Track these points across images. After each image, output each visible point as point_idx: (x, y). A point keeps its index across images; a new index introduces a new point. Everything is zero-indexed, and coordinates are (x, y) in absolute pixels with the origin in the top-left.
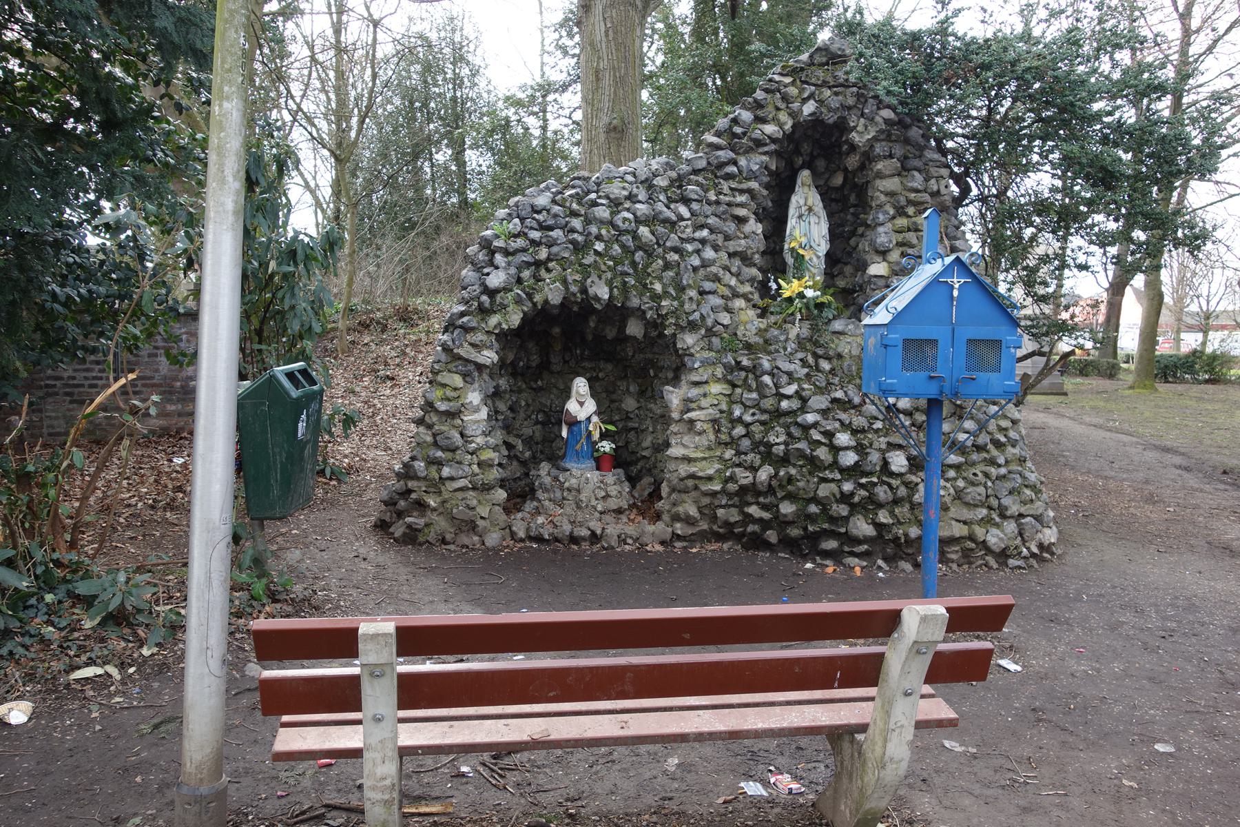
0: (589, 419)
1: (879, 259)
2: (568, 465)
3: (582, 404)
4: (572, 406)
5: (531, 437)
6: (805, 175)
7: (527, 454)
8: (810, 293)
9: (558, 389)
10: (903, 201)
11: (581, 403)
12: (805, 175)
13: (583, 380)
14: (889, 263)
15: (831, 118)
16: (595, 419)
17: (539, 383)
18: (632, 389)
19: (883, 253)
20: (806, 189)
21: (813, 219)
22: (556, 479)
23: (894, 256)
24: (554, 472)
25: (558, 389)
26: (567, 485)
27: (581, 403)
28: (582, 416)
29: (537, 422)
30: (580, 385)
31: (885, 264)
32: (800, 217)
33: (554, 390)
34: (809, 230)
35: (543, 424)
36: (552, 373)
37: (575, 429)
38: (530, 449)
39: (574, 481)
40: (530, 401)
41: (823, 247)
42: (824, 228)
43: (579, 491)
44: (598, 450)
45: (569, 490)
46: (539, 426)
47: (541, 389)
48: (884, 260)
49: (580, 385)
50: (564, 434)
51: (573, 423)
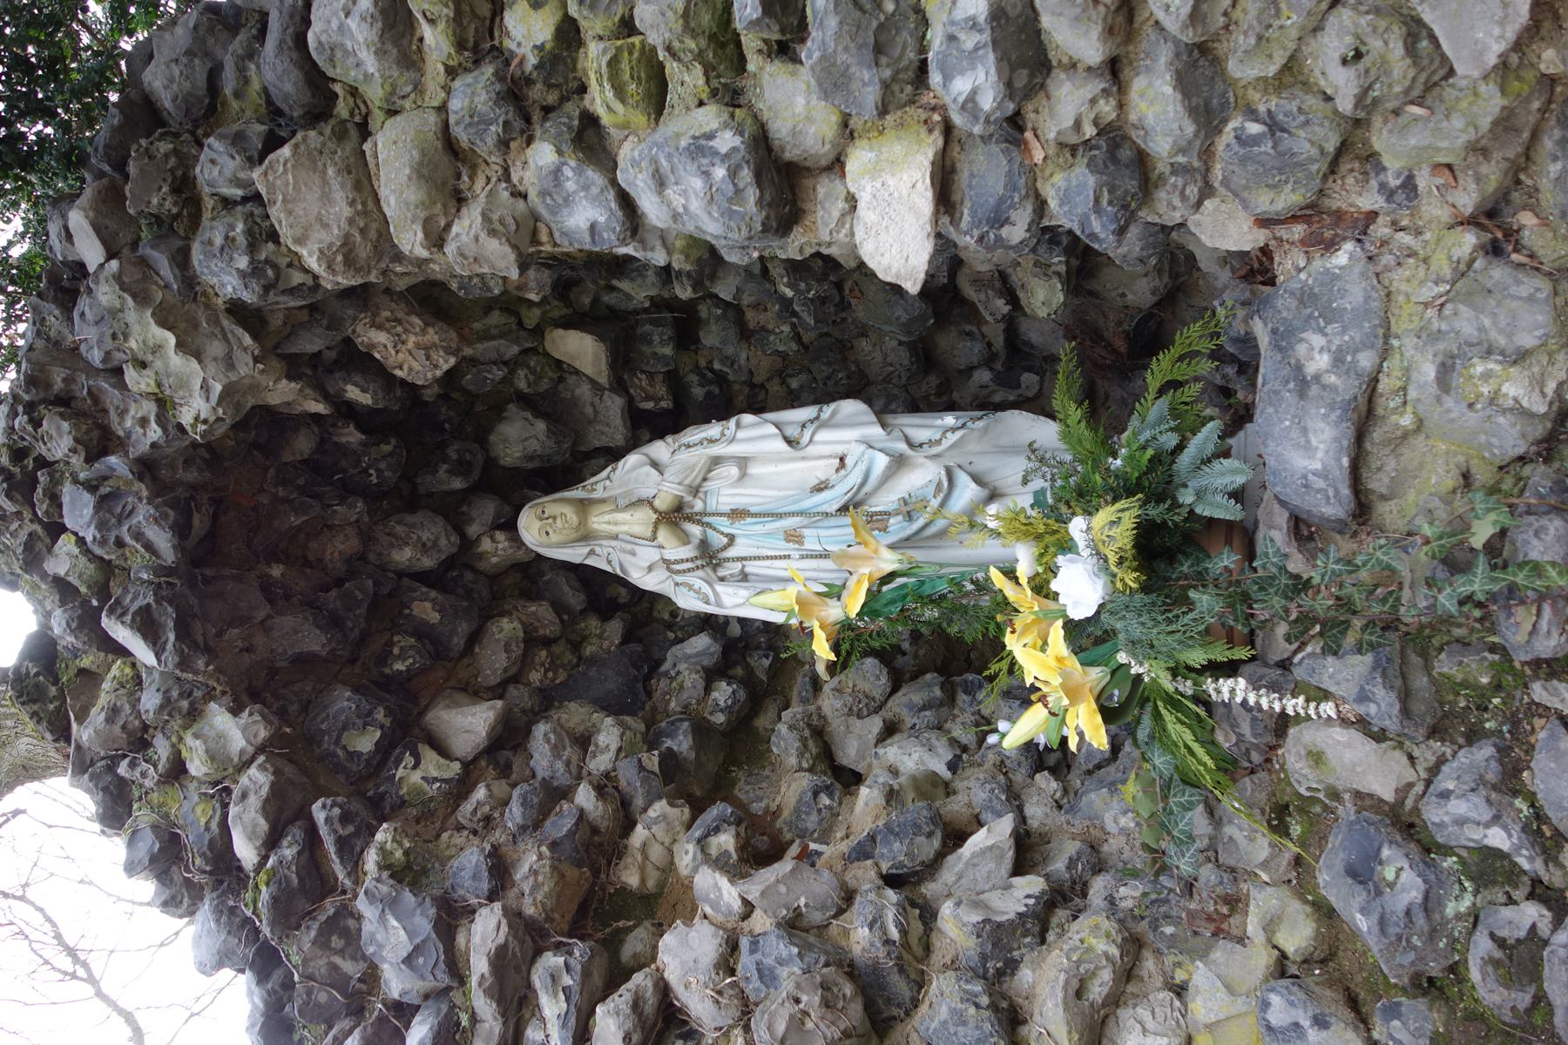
1: (826, 201)
6: (544, 529)
8: (1081, 589)
10: (473, 95)
12: (544, 529)
14: (848, 132)
15: (154, 535)
19: (784, 181)
20: (600, 521)
21: (724, 493)
23: (793, 103)
31: (858, 159)
32: (709, 557)
34: (773, 518)
41: (846, 437)
42: (752, 435)
48: (837, 165)
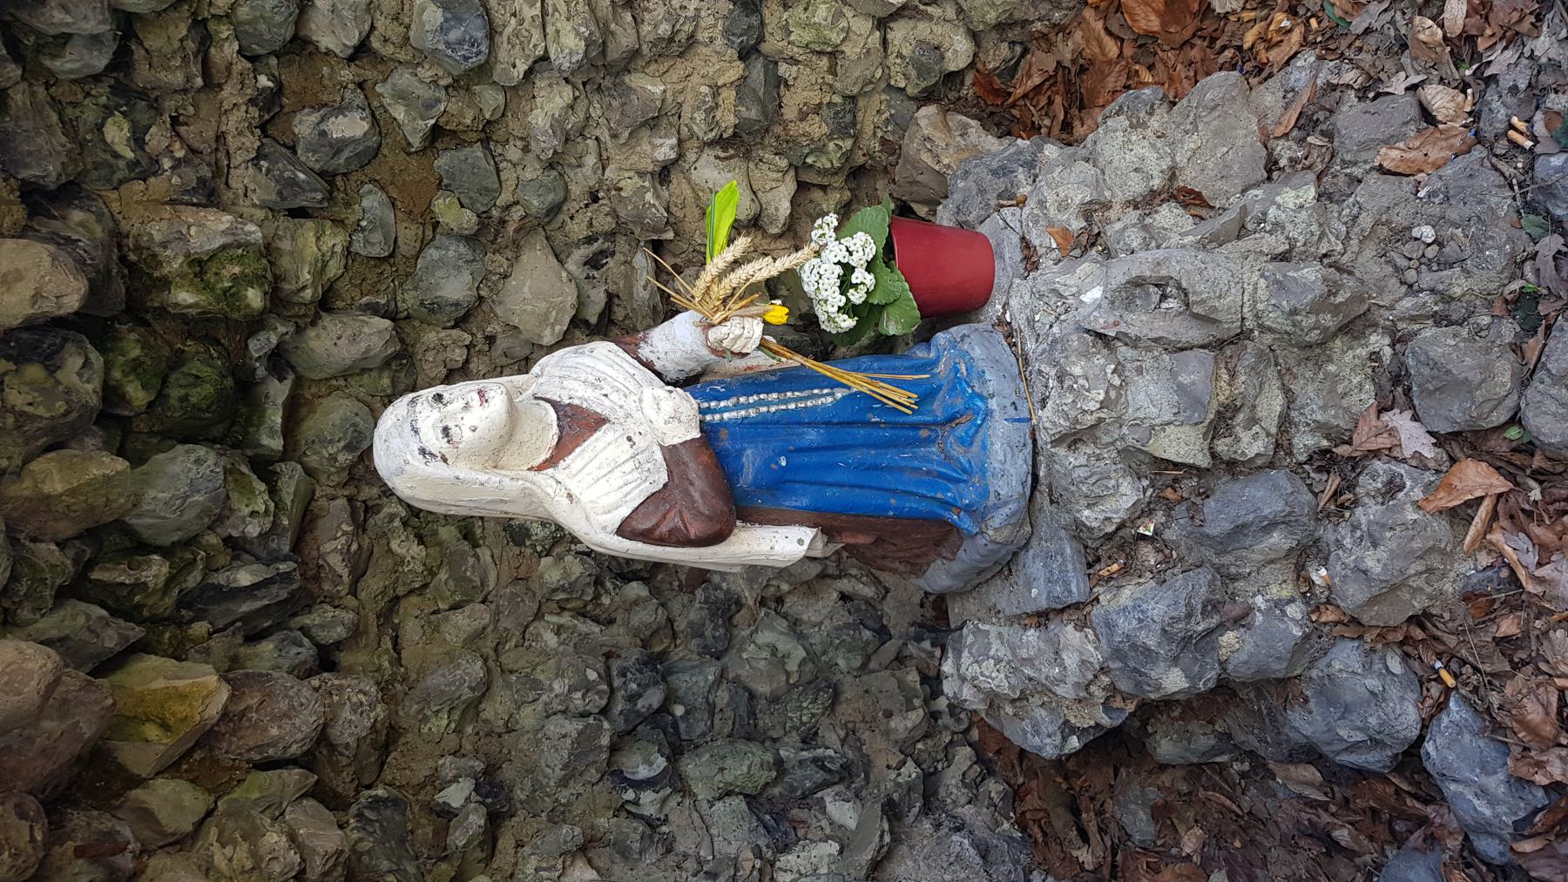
0: (688, 382)
2: (1004, 467)
3: (577, 424)
4: (598, 493)
5: (750, 799)
7: (842, 811)
9: (485, 689)
11: (568, 441)
13: (394, 415)
16: (676, 340)
17: (456, 795)
18: (455, 288)
22: (1110, 551)
24: (1038, 582)
25: (485, 689)
26: (1183, 445)
27: (568, 441)
28: (672, 417)
29: (673, 780)
30: (436, 443)
33: (495, 709)
35: (676, 750)
36: (387, 739)
37: (750, 462)
38: (808, 799)
39: (1150, 397)
40: (569, 833)
43: (1226, 344)
44: (866, 313)
45: (1222, 423)
46: (692, 767)
47: (490, 785)
49: (436, 443)
50: (784, 544)
51: (720, 478)
